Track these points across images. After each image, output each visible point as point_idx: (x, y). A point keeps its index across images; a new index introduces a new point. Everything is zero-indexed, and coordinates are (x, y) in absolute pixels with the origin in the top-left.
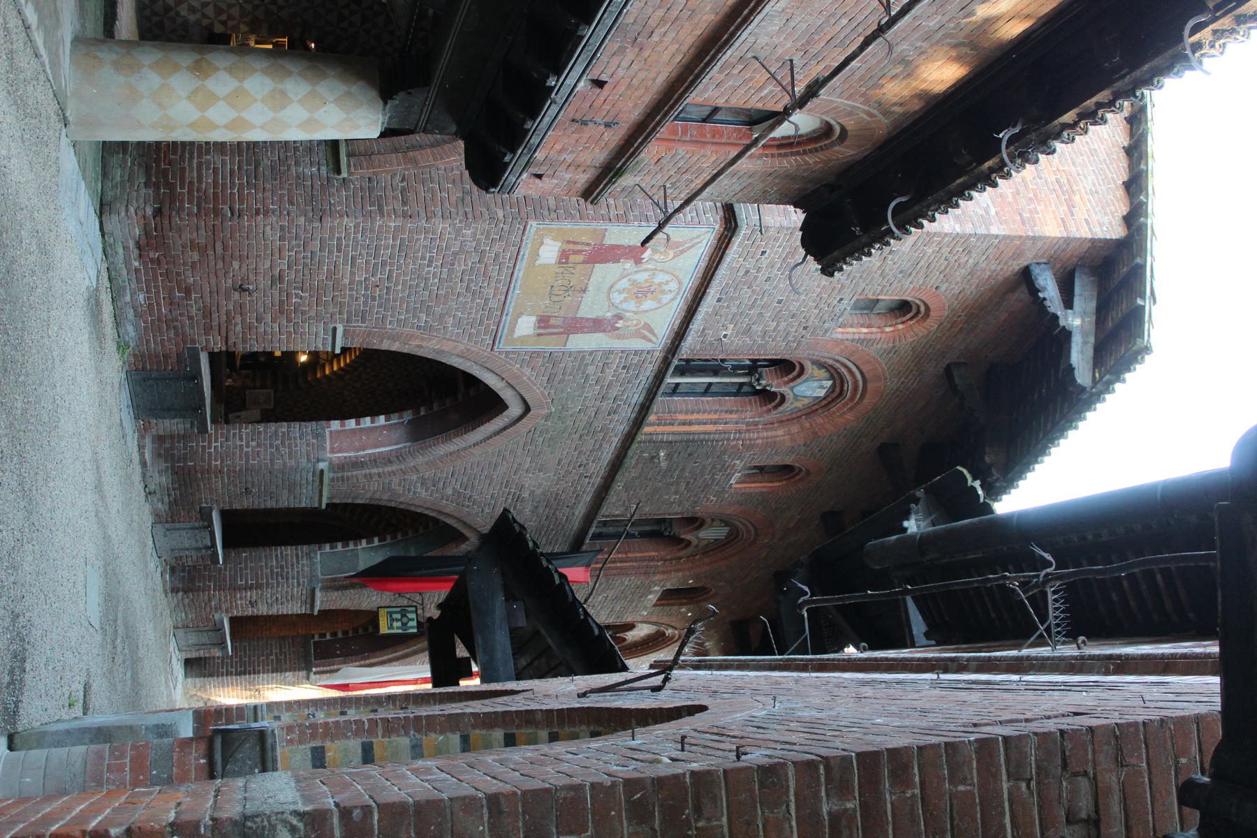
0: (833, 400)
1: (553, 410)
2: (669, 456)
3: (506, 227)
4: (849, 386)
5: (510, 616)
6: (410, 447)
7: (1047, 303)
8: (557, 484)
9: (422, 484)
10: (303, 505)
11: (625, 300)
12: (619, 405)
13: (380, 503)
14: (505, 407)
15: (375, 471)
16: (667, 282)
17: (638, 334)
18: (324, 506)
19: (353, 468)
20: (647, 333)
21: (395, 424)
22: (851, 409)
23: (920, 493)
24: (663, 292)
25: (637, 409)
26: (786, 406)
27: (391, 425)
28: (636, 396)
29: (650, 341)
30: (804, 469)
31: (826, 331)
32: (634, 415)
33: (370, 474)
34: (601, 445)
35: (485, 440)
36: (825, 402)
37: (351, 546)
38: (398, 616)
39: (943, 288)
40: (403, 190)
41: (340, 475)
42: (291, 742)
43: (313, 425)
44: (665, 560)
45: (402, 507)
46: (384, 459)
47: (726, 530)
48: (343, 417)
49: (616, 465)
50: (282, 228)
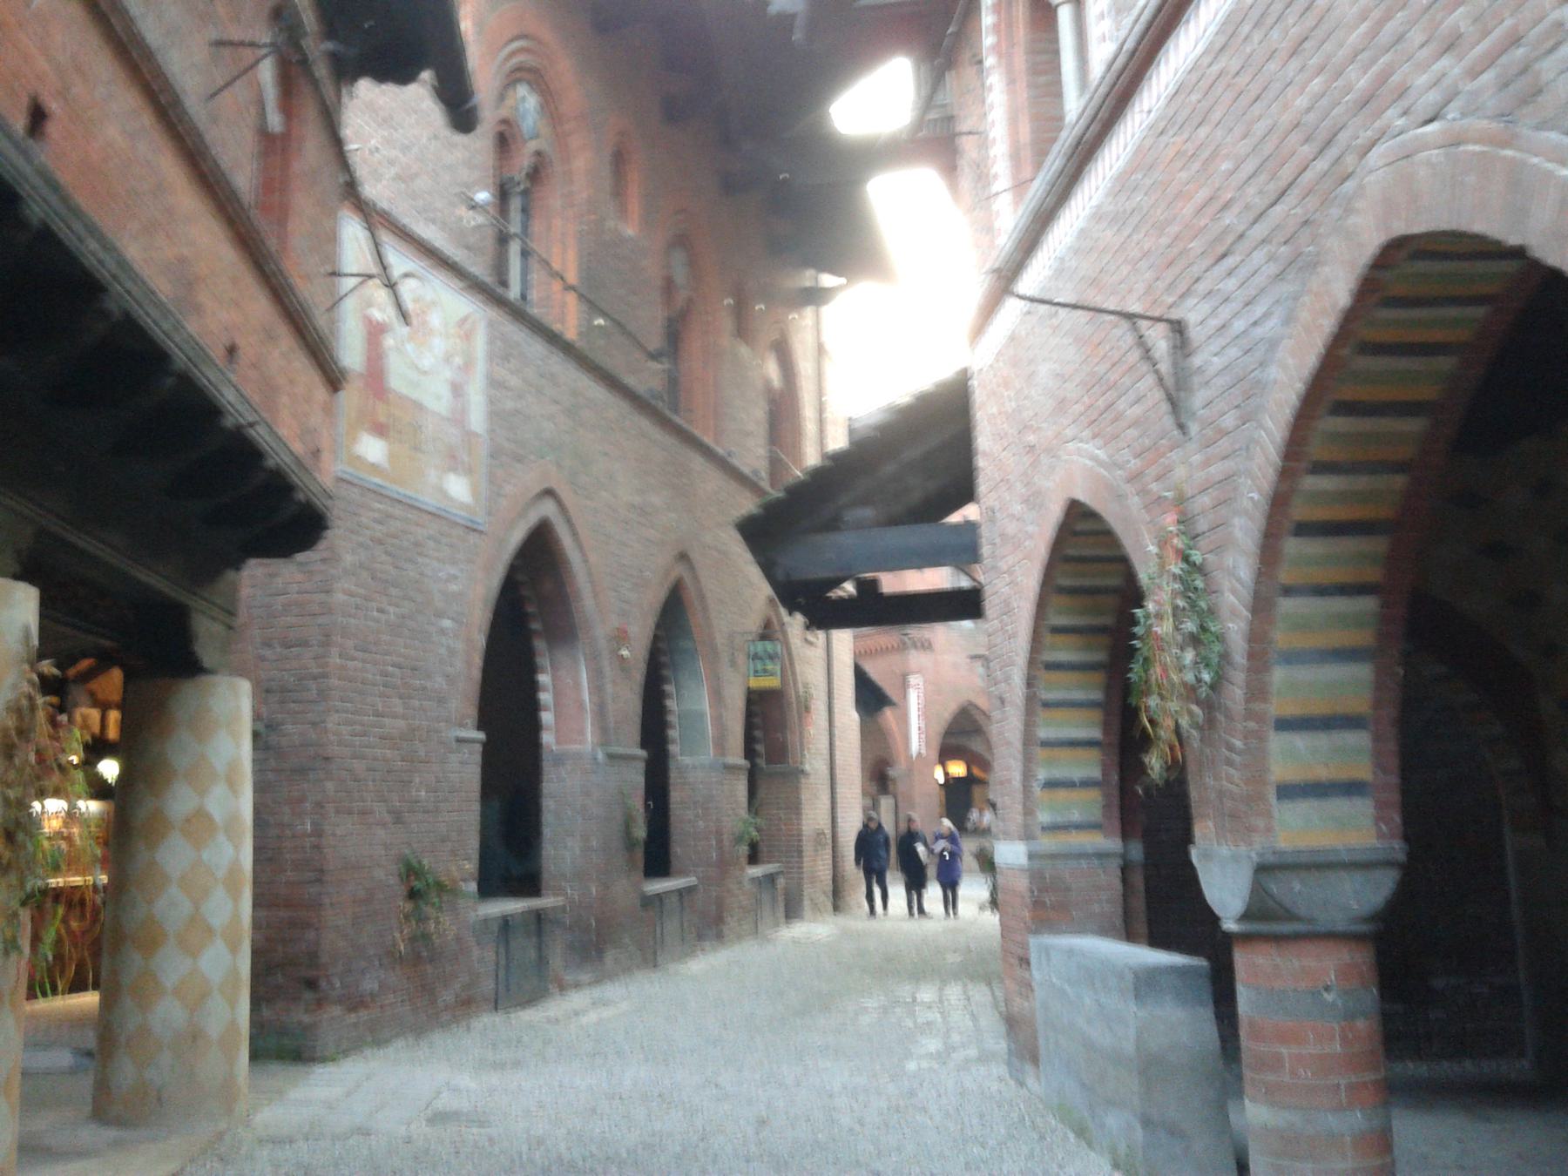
15: (609, 688)
17: (468, 337)
27: (551, 666)
35: (580, 547)
40: (287, 645)
42: (1269, 830)
48: (535, 727)
49: (611, 381)
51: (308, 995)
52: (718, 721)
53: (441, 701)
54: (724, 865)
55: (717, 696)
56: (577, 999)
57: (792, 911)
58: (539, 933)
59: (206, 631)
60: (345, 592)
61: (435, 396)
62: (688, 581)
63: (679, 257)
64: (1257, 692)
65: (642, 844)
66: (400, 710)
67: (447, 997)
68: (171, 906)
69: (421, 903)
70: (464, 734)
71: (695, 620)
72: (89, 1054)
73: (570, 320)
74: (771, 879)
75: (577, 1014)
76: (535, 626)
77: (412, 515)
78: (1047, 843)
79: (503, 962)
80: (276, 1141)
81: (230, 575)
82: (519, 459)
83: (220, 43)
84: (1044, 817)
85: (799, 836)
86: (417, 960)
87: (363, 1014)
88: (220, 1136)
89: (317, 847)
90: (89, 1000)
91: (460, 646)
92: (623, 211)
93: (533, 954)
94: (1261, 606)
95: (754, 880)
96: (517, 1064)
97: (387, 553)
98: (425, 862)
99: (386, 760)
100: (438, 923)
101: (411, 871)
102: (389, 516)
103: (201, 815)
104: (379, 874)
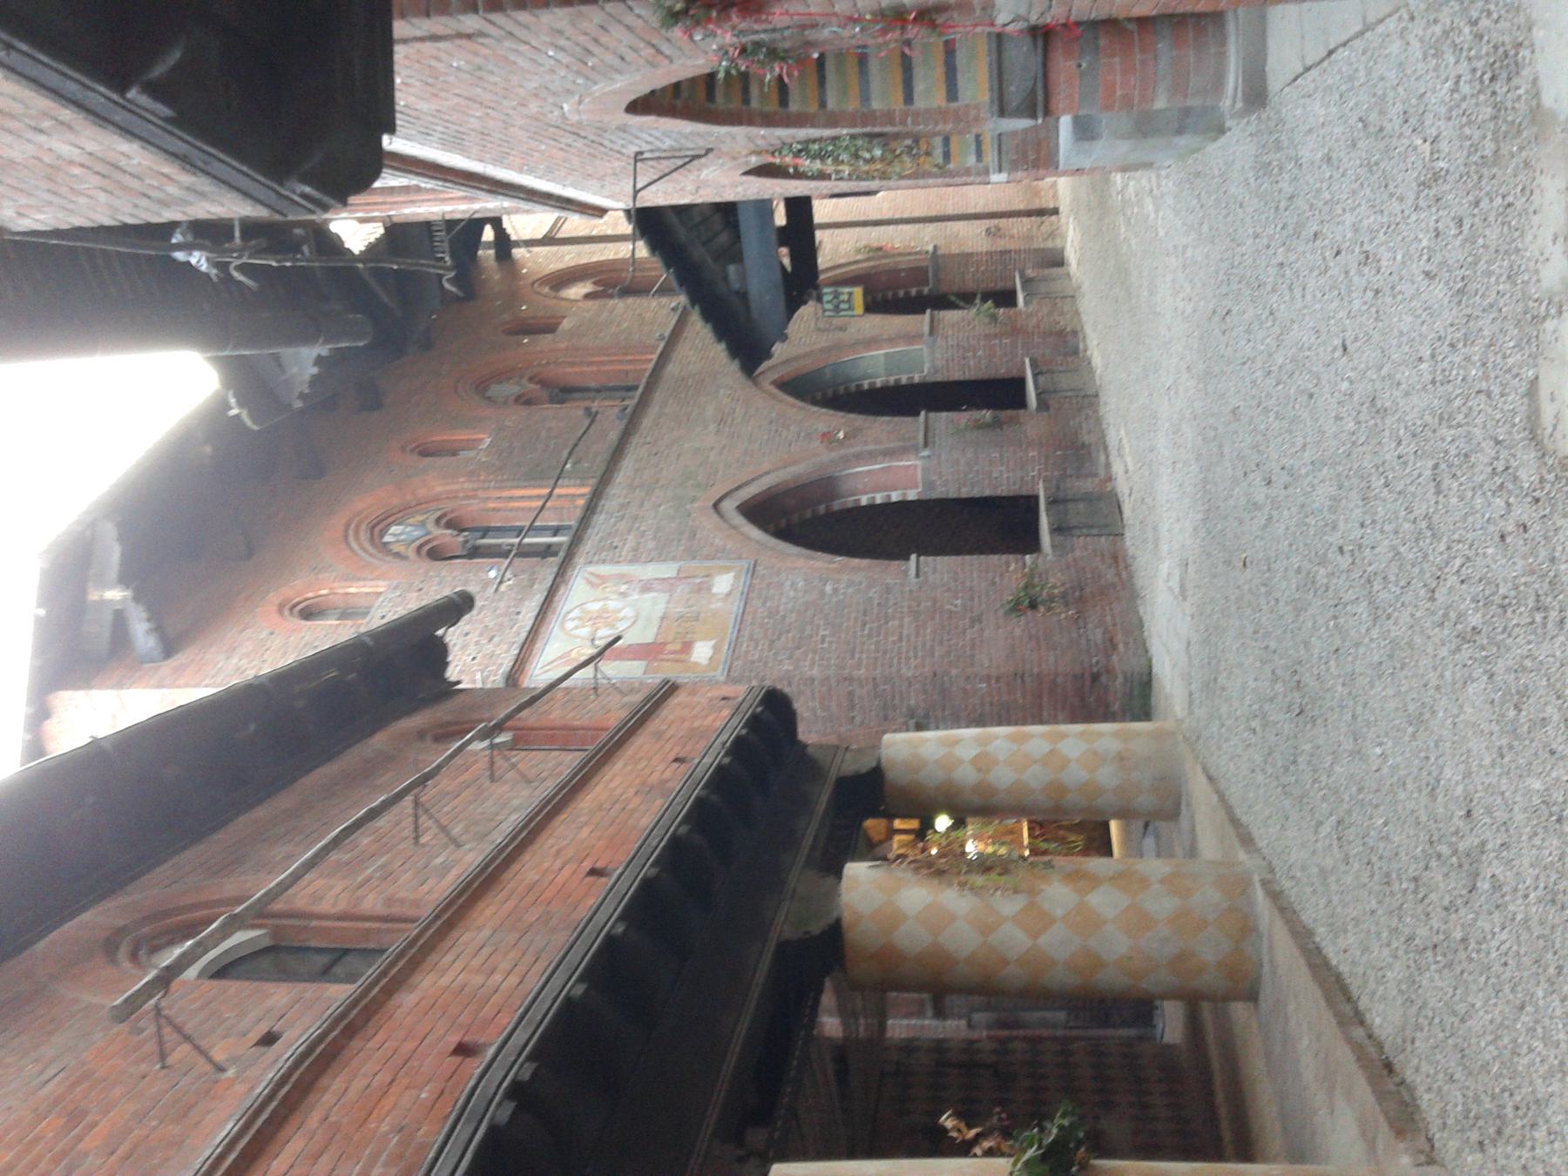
3: (747, 674)
4: (364, 536)
5: (743, 277)
7: (144, 615)
10: (944, 414)
11: (619, 611)
15: (871, 447)
16: (576, 628)
17: (603, 579)
18: (923, 413)
20: (598, 581)
22: (359, 514)
23: (298, 404)
24: (580, 619)
25: (599, 509)
29: (592, 574)
31: (396, 587)
32: (603, 502)
37: (892, 380)
38: (843, 306)
39: (264, 634)
40: (853, 707)
42: (977, 107)
43: (935, 495)
45: (841, 414)
47: (489, 394)
48: (904, 505)
50: (972, 665)
51: (1104, 679)
52: (891, 341)
53: (888, 590)
54: (1015, 331)
55: (871, 343)
56: (1117, 468)
57: (1056, 260)
58: (1065, 501)
59: (852, 765)
60: (811, 669)
61: (654, 605)
63: (495, 390)
64: (889, 117)
65: (998, 413)
66: (897, 623)
67: (1110, 575)
68: (1035, 778)
69: (1040, 599)
70: (913, 572)
71: (808, 365)
72: (1146, 826)
73: (575, 492)
74: (1027, 282)
75: (1127, 472)
76: (822, 509)
77: (748, 618)
78: (990, 157)
79: (1085, 531)
80: (1191, 703)
81: (810, 750)
82: (693, 535)
83: (492, 778)
84: (971, 160)
85: (990, 254)
86: (1081, 600)
87: (1119, 637)
88: (1186, 739)
89: (998, 679)
90: (1114, 826)
91: (845, 577)
92: (471, 445)
93: (1081, 506)
94: (833, 121)
95: (1026, 303)
96: (1155, 529)
97: (779, 639)
98: (1010, 598)
99: (934, 632)
100: (1054, 587)
101: (1016, 608)
102: (751, 638)
103: (975, 761)
104: (1018, 631)
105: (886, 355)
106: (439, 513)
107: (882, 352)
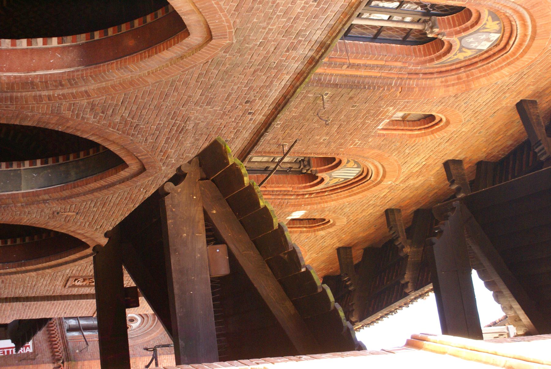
0: (494, 54)
1: (234, 42)
2: (332, 98)
6: (82, 70)
8: (221, 118)
9: (92, 109)
12: (300, 41)
13: (47, 127)
14: (188, 34)
15: (45, 93)
19: (23, 88)
21: (69, 47)
26: (455, 56)
27: (64, 47)
28: (319, 32)
30: (444, 120)
33: (40, 96)
34: (271, 82)
36: (486, 55)
37: (15, 167)
41: (9, 95)
44: (298, 195)
45: (69, 131)
46: (55, 81)
62: (124, 174)
76: (97, 35)
105: (21, 190)
106: (444, 59)
107: (22, 191)
